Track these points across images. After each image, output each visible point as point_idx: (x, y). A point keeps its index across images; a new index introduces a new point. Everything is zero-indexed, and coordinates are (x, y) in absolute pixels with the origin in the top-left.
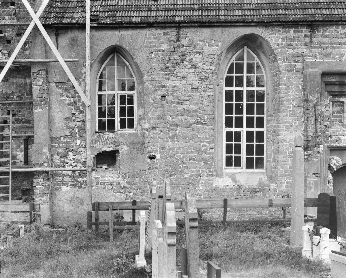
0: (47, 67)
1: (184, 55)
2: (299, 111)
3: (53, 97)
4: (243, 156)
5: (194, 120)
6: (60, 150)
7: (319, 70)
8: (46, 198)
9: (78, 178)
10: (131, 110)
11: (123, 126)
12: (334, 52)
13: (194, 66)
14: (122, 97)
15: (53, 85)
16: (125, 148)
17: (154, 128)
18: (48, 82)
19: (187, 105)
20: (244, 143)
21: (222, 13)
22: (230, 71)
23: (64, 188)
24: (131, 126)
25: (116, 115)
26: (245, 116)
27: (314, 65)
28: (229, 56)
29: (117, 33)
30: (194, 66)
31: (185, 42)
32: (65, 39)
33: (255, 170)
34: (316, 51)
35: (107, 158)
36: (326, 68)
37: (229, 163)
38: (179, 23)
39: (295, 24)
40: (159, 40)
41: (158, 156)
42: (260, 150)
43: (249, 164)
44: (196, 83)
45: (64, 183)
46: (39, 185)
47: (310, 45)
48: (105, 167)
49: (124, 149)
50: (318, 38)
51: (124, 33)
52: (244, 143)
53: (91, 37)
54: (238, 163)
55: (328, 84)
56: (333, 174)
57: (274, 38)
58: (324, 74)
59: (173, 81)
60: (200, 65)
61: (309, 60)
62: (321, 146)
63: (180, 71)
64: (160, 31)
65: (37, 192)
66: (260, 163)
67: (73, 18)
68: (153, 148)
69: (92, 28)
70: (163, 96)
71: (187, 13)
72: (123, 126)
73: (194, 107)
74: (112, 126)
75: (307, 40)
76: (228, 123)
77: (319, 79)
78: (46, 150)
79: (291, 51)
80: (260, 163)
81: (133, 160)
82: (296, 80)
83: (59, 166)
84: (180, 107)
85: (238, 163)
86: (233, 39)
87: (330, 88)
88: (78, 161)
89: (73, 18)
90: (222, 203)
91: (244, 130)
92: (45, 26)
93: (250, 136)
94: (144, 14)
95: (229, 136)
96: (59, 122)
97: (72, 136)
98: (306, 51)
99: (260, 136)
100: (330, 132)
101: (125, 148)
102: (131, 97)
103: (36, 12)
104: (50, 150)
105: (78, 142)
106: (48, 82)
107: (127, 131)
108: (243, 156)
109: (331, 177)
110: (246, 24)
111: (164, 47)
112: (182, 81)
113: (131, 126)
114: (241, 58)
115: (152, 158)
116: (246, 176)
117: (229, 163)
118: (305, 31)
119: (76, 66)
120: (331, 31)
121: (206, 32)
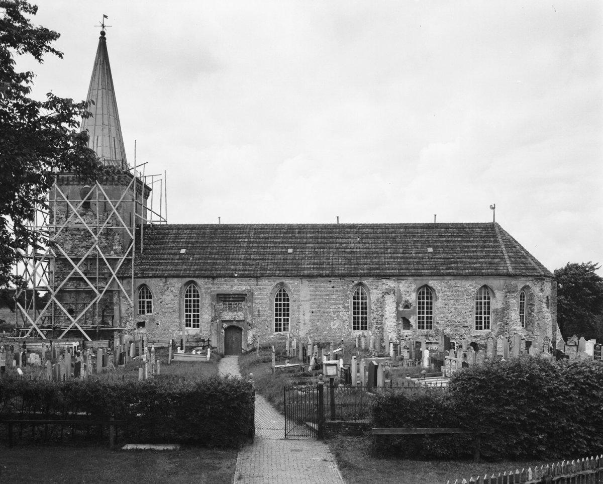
0: (119, 292)
1: (168, 287)
2: (210, 308)
3: (122, 302)
4: (192, 323)
5: (172, 310)
6: (124, 321)
7: (216, 293)
8: (118, 339)
9: (130, 332)
10: (151, 306)
11: (148, 312)
12: (221, 287)
13: (172, 291)
14: (148, 302)
15: (121, 298)
16: (148, 321)
17: (158, 313)
18: (119, 297)
19: (169, 305)
20: (192, 319)
21: (182, 272)
22: (187, 292)
23: (125, 335)
24: (151, 312)
25: (144, 308)
26: (192, 309)
27: (214, 291)
28: (186, 287)
29: (144, 279)
30: (172, 291)
31: (168, 283)
32: (125, 282)
33: (196, 328)
34: (215, 286)
35: (141, 324)
36: (218, 293)
37: (187, 326)
38: (166, 276)
39: (207, 277)
40: (160, 283)
41: (159, 324)
42: (198, 321)
43: (194, 326)
44: (173, 297)
45: (126, 334)
46: (116, 334)
47: (213, 284)
48: (141, 327)
49: (147, 321)
50: (215, 282)
51: (146, 279)
52: (192, 319)
53: (134, 281)
54: (190, 326)
55: (220, 298)
56: (225, 330)
57: (200, 282)
58: (218, 295)
59: (164, 297)
60: (174, 291)
61: (213, 289)
62: (218, 320)
63: (166, 293)
64: (159, 279)
65: (115, 337)
66: (198, 326)
67: (128, 274)
68: (158, 320)
69: (134, 278)
70: (161, 302)
71: (170, 272)
72: (148, 312)
73: (172, 306)
74: (144, 313)
75: (212, 282)
76: (186, 311)
77: (216, 297)
78: (118, 322)
79: (206, 286)
80: (198, 326)
81: (150, 325)
82: (208, 296)
83: (124, 327)
84: (167, 306)
85: (190, 326)
86: (185, 282)
87: (221, 299)
88: (131, 326)
89: (128, 274)
90: (180, 340)
91: (192, 314)
92: (118, 277)
93: (194, 316)
94: (154, 272)
95: (187, 315)
96: (123, 311)
97: (128, 316)
98: (211, 286)
99: (198, 316)
100: (222, 314)
101: (148, 321)
102: (150, 302)
103: (114, 272)
104: (120, 321)
105: (131, 318)
106: (119, 297)
107: (149, 314)
108: (192, 323)
109: (223, 331)
110: (189, 277)
111: (161, 284)
112: (168, 297)
113: (151, 312)
114: (190, 287)
115: (158, 324)
116: (192, 331)
117: (187, 326)
118: (211, 279)
119: (128, 292)
120: (219, 279)
121: (176, 280)
